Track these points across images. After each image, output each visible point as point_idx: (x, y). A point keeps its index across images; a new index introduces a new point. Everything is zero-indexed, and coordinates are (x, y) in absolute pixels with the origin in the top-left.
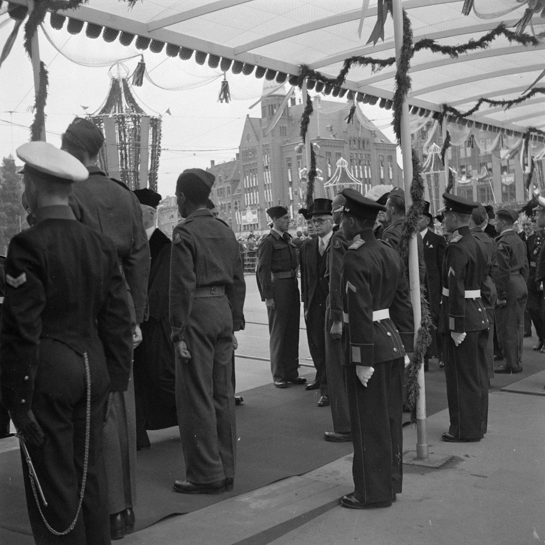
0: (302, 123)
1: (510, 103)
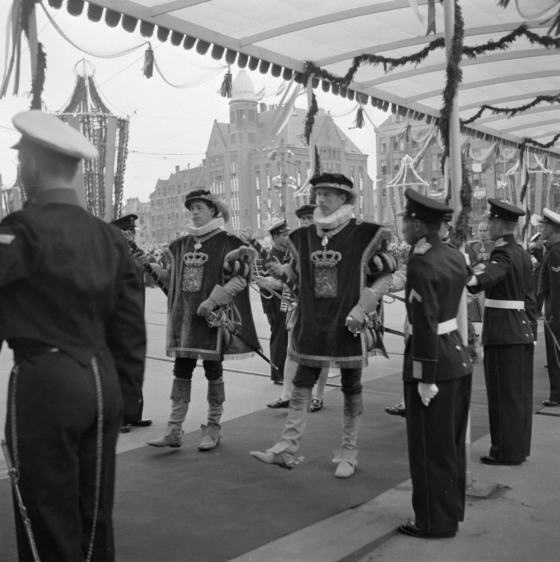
0: (307, 124)
1: (514, 111)
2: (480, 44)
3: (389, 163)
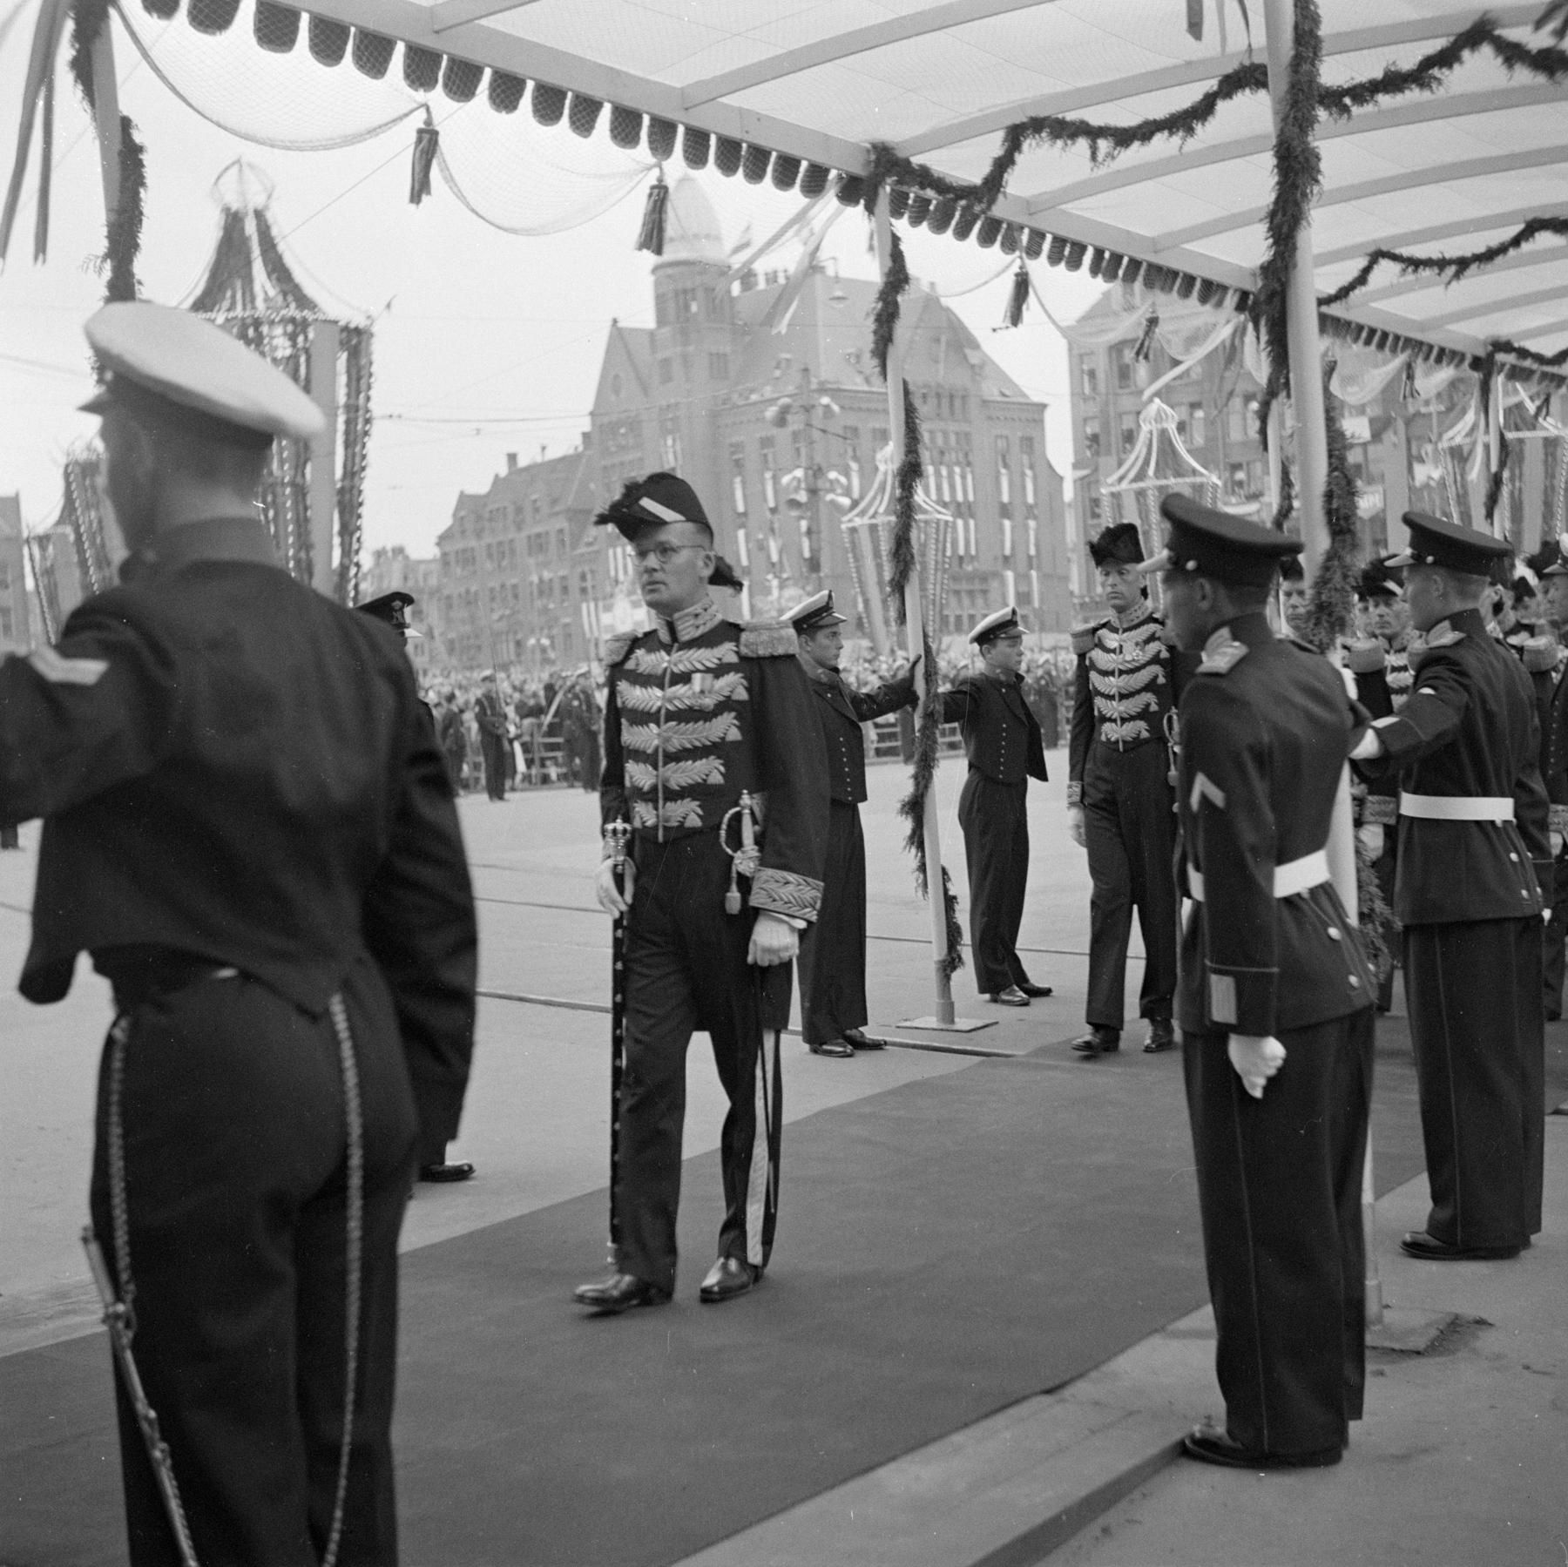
0: (879, 319)
1: (1463, 264)
3: (1106, 425)
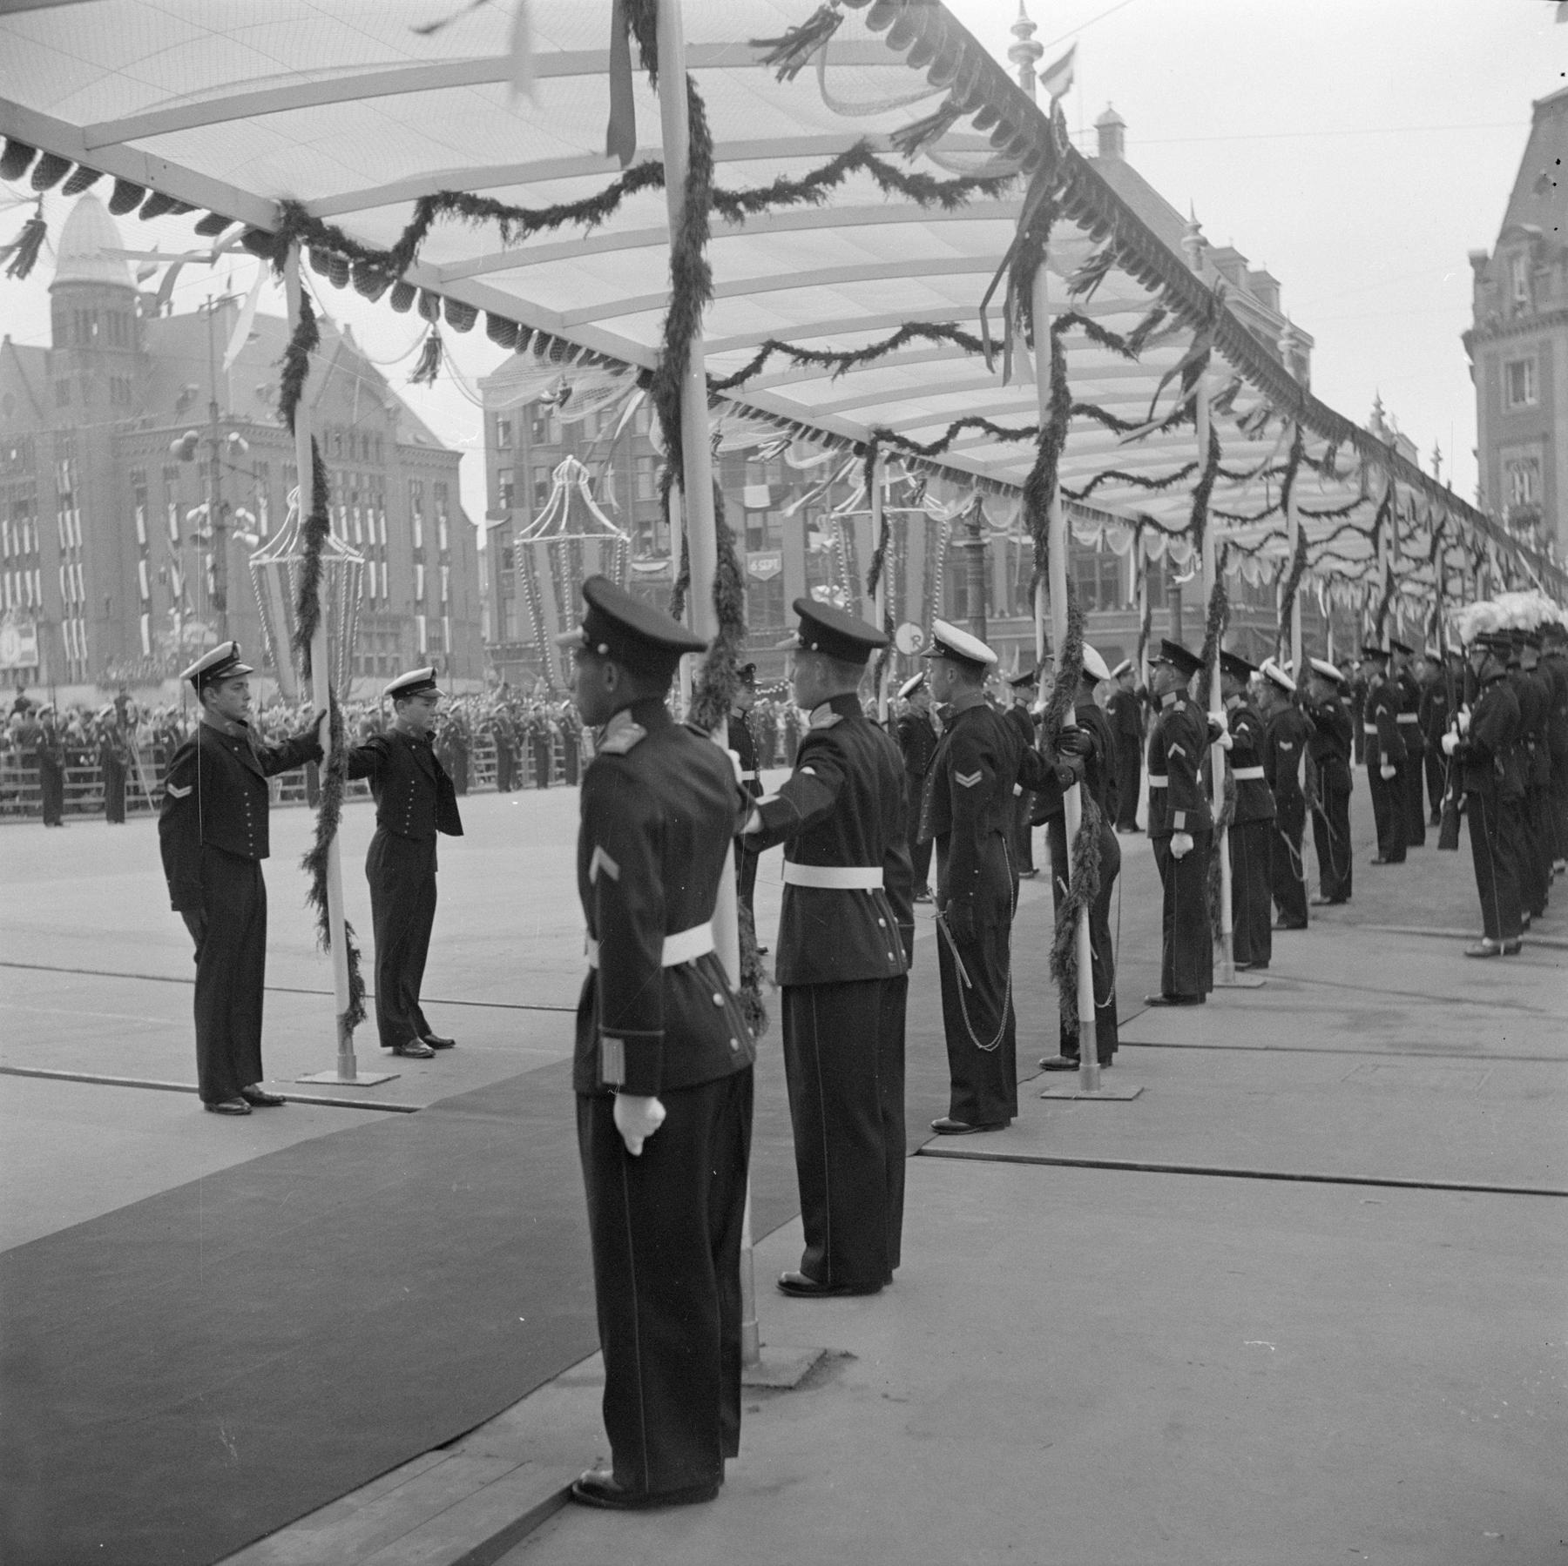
1: (847, 360)
2: (755, 185)
3: (519, 479)
